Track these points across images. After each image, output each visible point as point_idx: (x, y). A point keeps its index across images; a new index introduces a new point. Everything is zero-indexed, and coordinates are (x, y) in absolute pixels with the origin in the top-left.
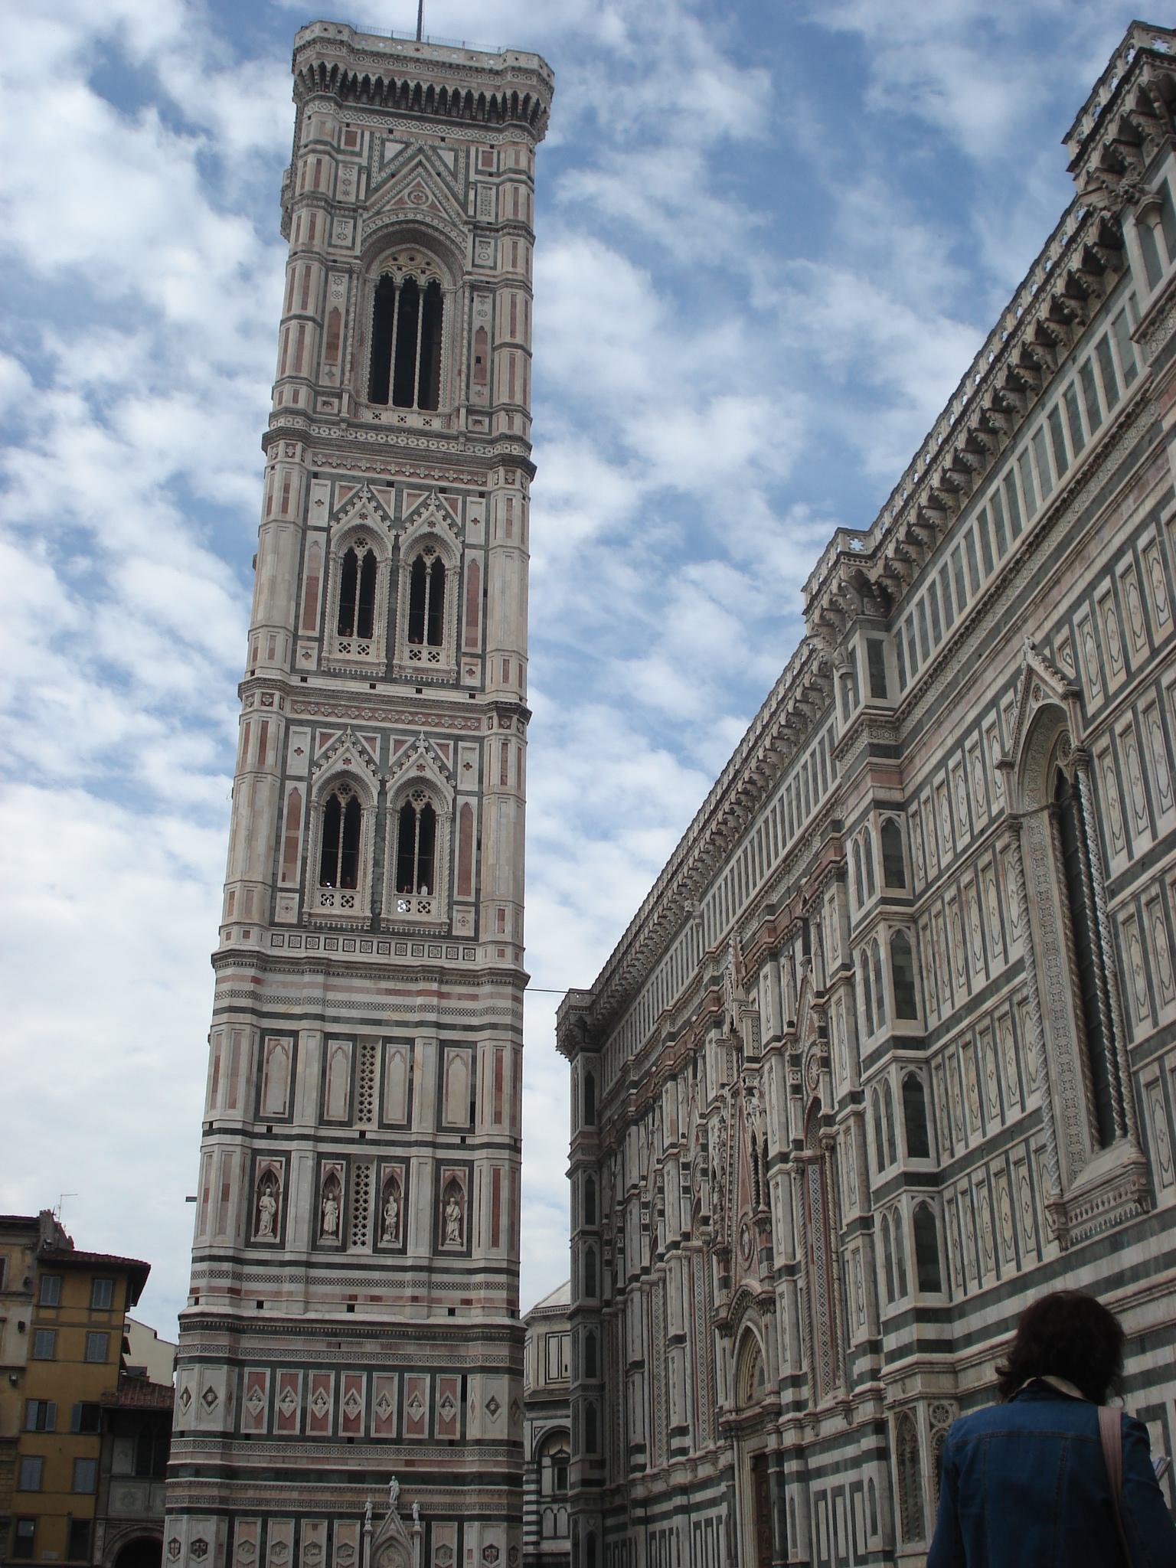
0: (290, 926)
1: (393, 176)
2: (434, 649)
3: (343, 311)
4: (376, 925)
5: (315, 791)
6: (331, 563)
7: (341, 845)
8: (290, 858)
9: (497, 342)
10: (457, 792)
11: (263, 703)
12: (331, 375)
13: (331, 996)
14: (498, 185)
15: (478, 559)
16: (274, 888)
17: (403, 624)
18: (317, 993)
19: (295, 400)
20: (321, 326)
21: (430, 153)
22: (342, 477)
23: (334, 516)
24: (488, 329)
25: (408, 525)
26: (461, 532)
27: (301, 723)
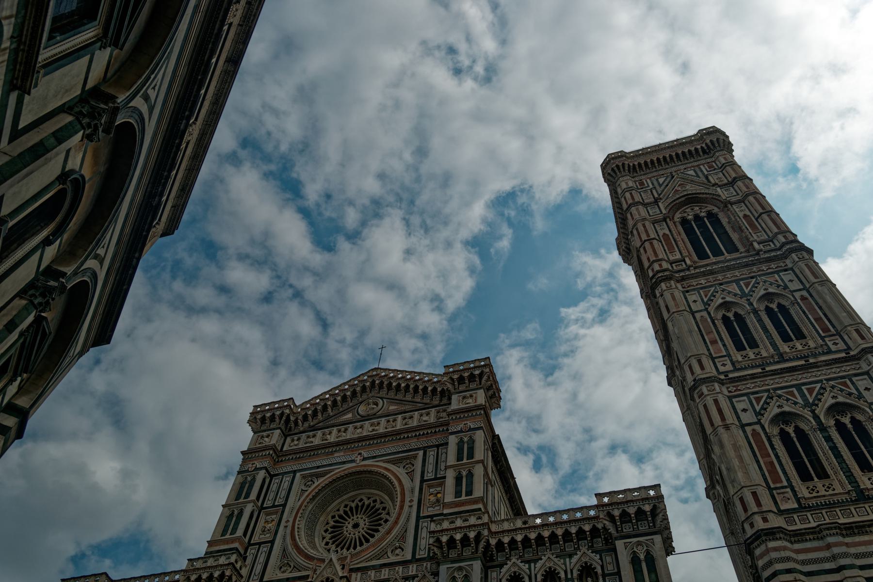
0: (794, 509)
5: (766, 426)
6: (716, 321)
7: (803, 454)
9: (756, 215)
11: (709, 391)
13: (853, 550)
14: (722, 171)
15: (803, 294)
18: (844, 549)
20: (661, 242)
22: (702, 288)
23: (705, 304)
24: (748, 213)
25: (751, 293)
26: (786, 287)
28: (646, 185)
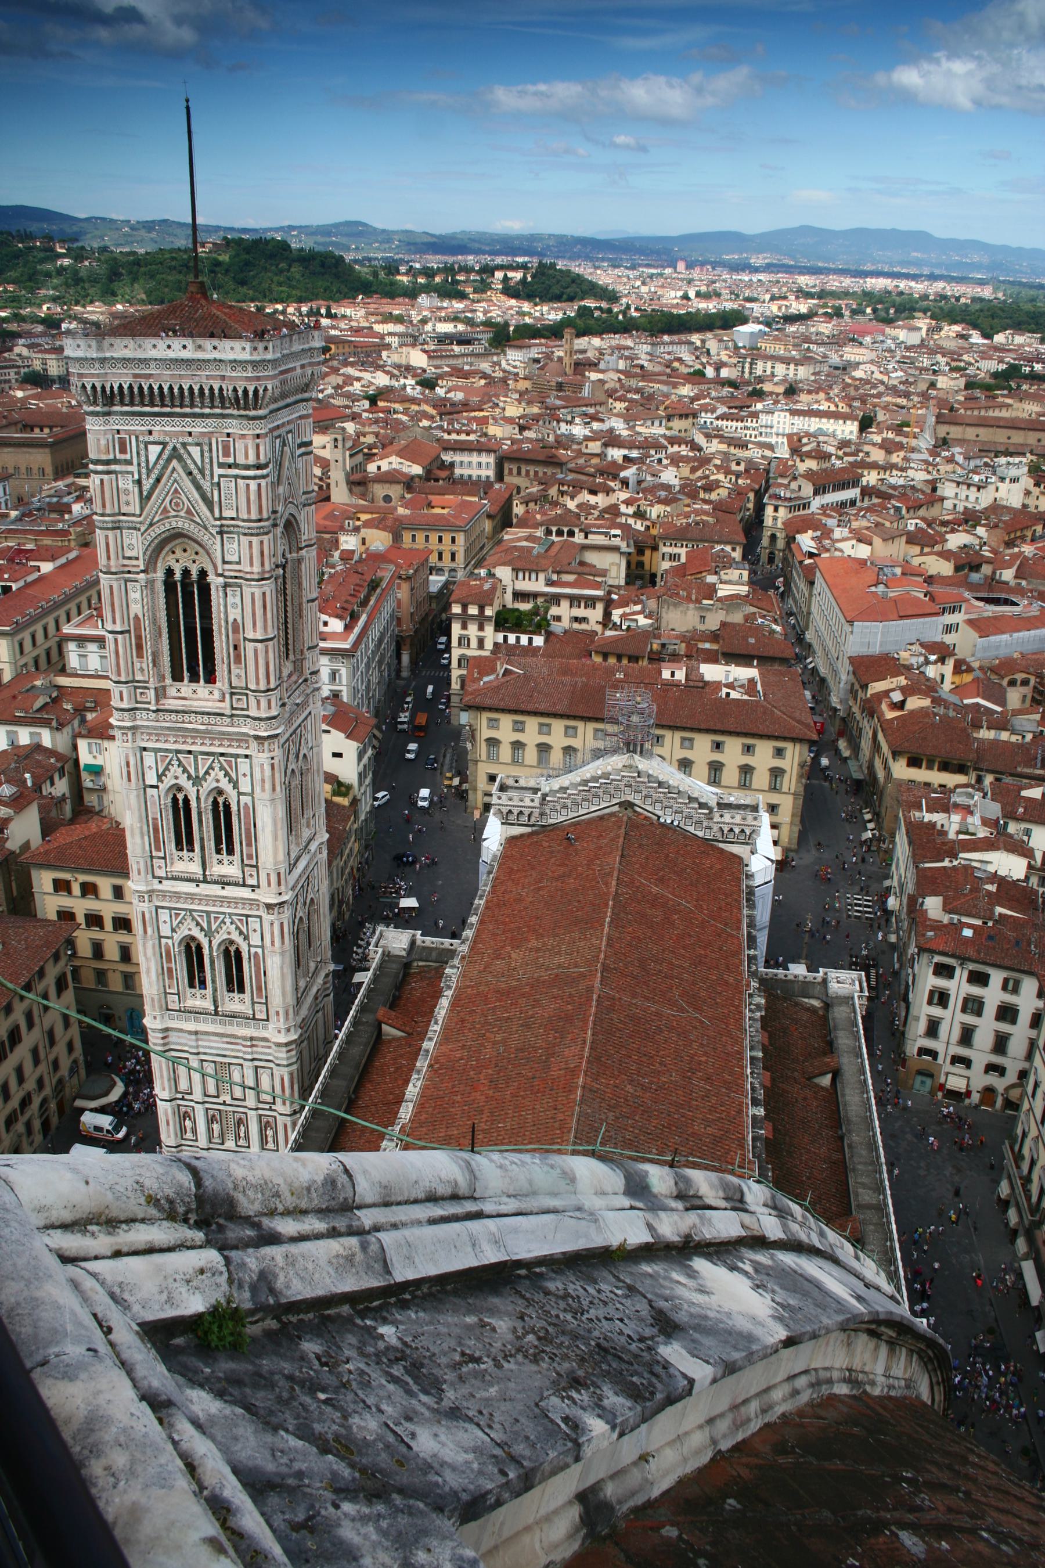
1: (158, 480)
2: (231, 858)
3: (141, 616)
4: (216, 1013)
8: (171, 977)
10: (249, 946)
12: (142, 670)
16: (166, 993)
17: (210, 844)
18: (194, 1044)
19: (122, 699)
21: (182, 451)
22: (160, 750)
24: (239, 621)
26: (236, 786)
27: (163, 908)
28: (128, 457)
